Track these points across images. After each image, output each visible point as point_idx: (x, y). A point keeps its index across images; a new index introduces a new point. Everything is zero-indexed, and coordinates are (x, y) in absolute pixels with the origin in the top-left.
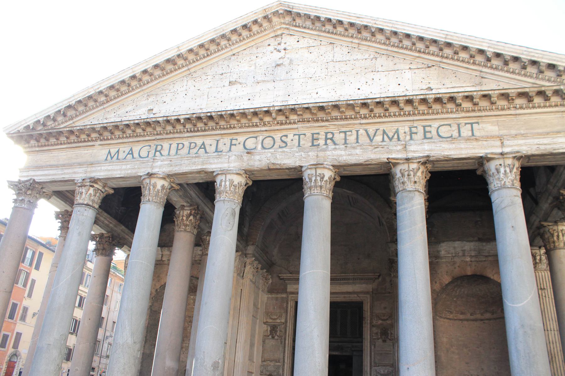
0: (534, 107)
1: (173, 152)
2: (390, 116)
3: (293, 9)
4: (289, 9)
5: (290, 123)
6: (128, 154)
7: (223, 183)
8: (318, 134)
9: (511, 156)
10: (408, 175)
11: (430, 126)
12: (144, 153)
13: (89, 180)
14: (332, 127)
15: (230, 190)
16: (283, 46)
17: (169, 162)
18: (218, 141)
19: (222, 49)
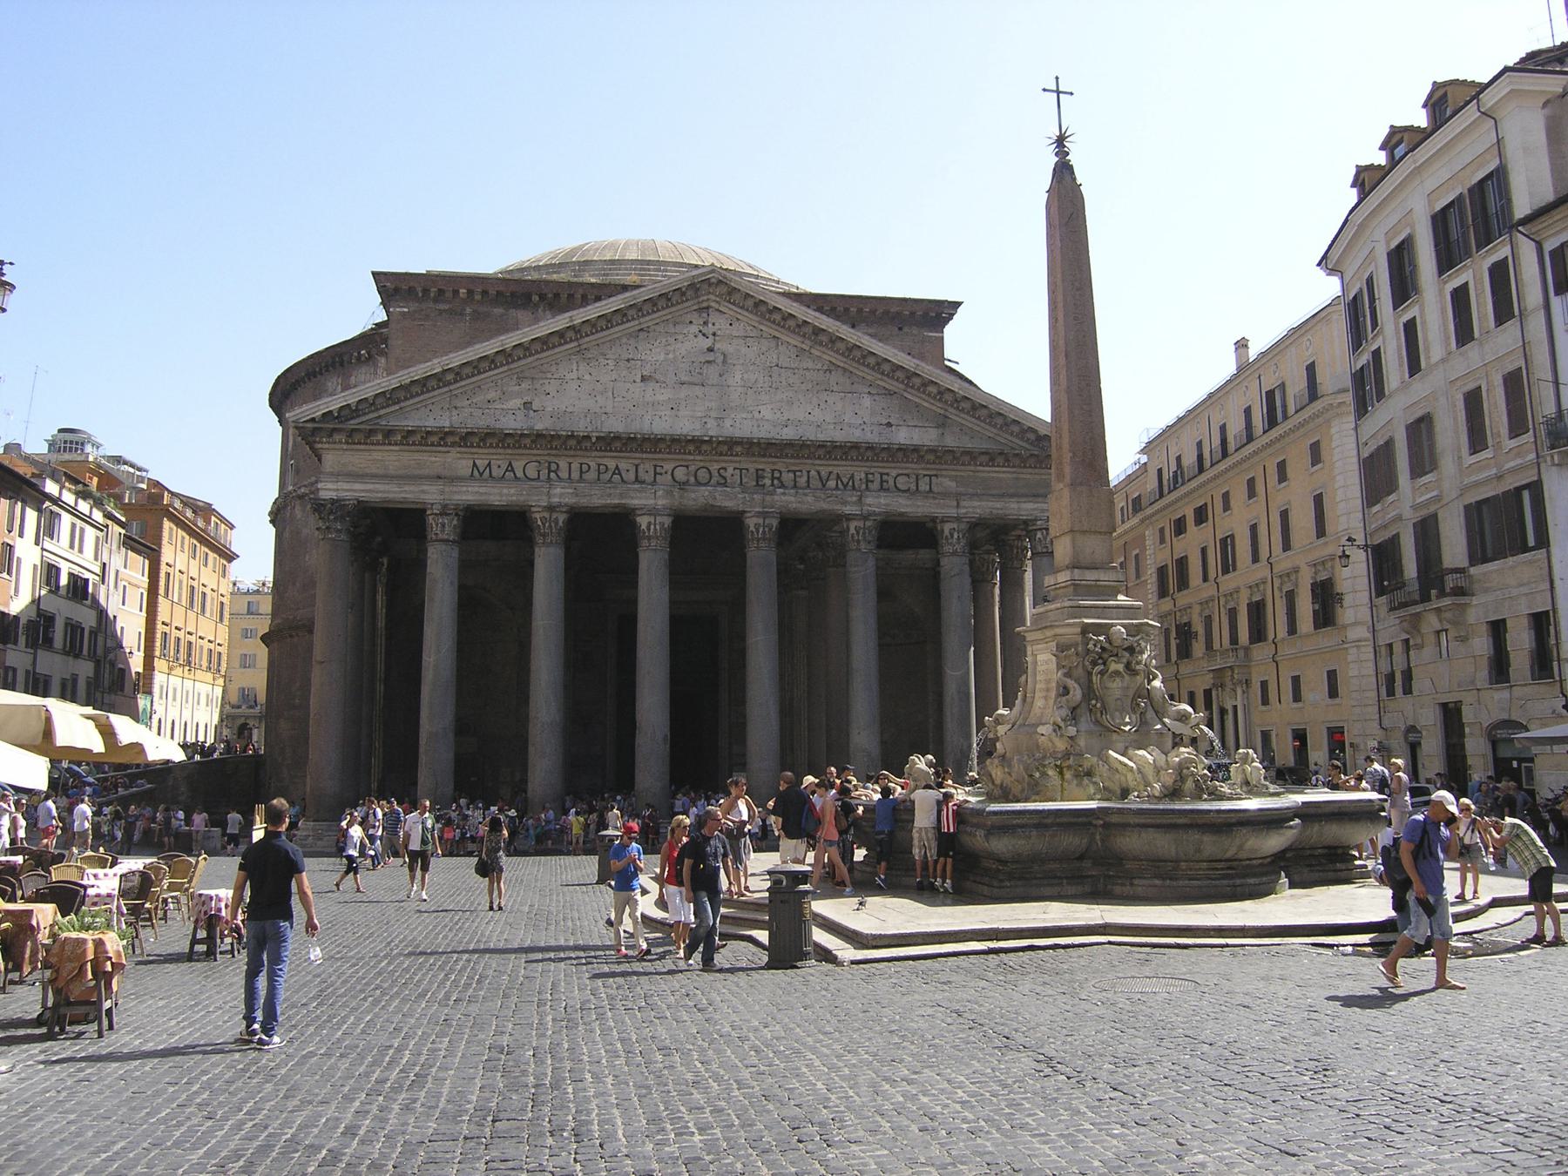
0: (993, 466)
1: (575, 475)
2: (846, 459)
5: (732, 455)
6: (507, 470)
7: (652, 527)
8: (763, 470)
10: (864, 533)
11: (887, 474)
12: (532, 473)
14: (780, 464)
15: (661, 536)
16: (710, 329)
17: (570, 491)
18: (637, 466)
19: (628, 321)
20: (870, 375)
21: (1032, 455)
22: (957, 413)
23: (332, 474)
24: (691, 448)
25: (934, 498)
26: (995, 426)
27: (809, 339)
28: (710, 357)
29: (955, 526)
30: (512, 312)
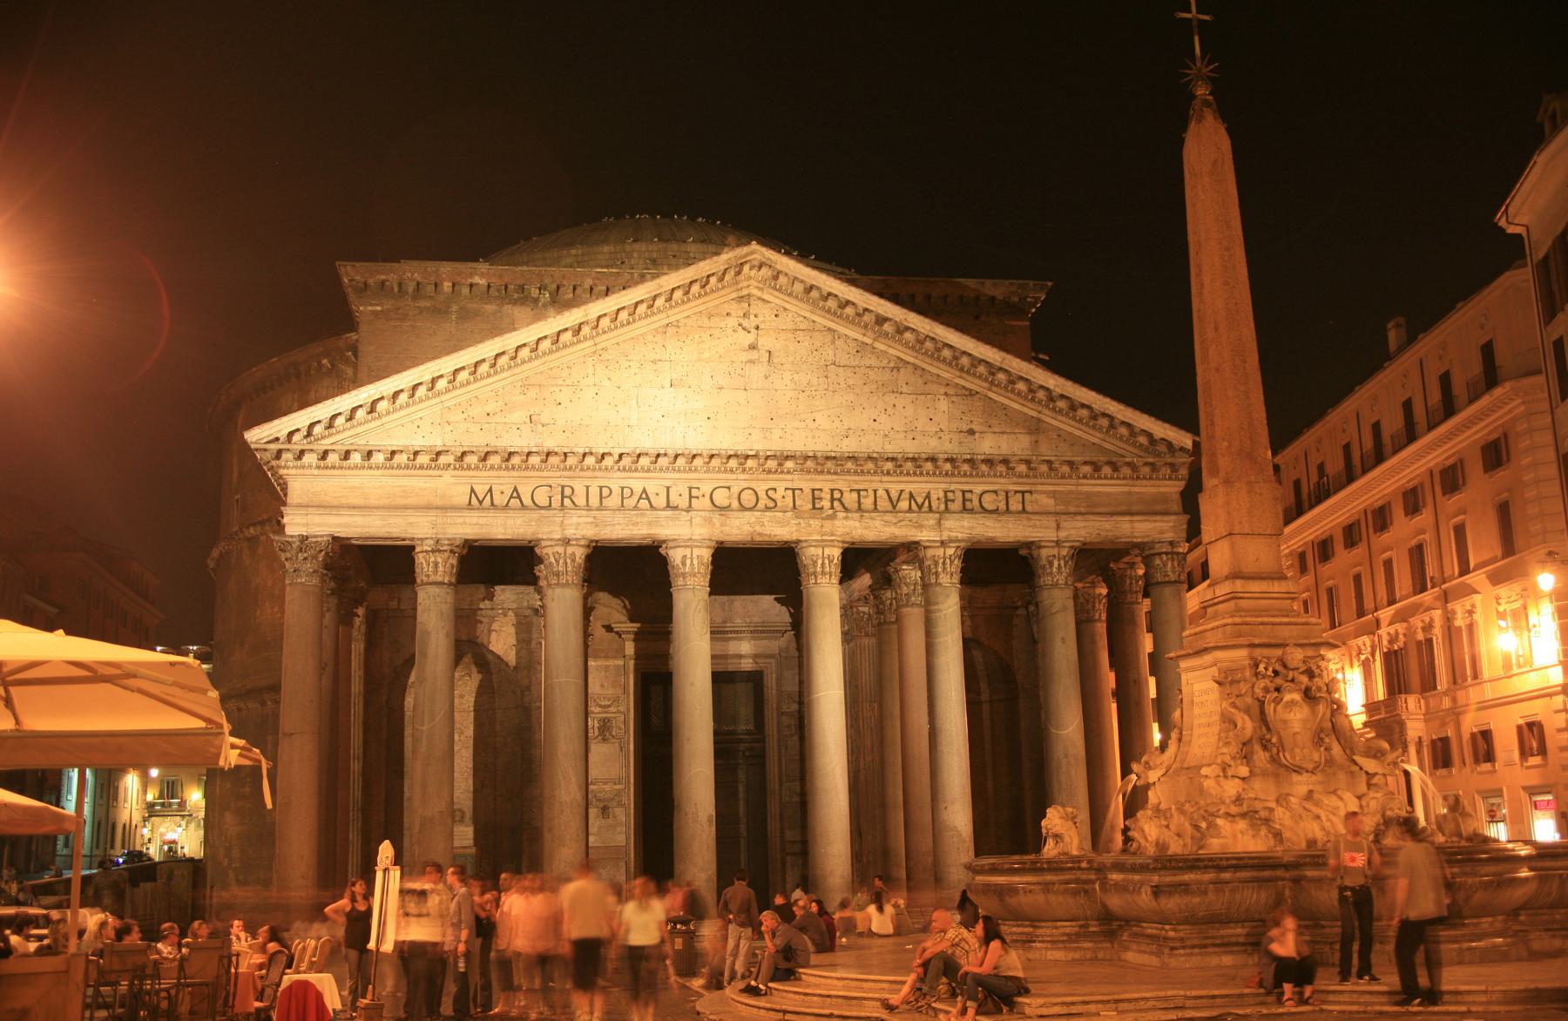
0: (1099, 478)
1: (594, 501)
2: (921, 474)
3: (776, 263)
4: (769, 262)
5: (782, 472)
6: (511, 497)
7: (688, 562)
8: (821, 490)
9: (1068, 544)
10: (944, 563)
11: (971, 491)
12: (541, 499)
13: (446, 542)
14: (841, 482)
16: (753, 321)
18: (668, 488)
19: (653, 314)
20: (946, 374)
21: (1146, 464)
22: (1054, 415)
23: (300, 506)
24: (733, 463)
25: (1029, 519)
26: (1100, 429)
27: (873, 330)
28: (754, 355)
29: (1055, 551)
30: (508, 308)
